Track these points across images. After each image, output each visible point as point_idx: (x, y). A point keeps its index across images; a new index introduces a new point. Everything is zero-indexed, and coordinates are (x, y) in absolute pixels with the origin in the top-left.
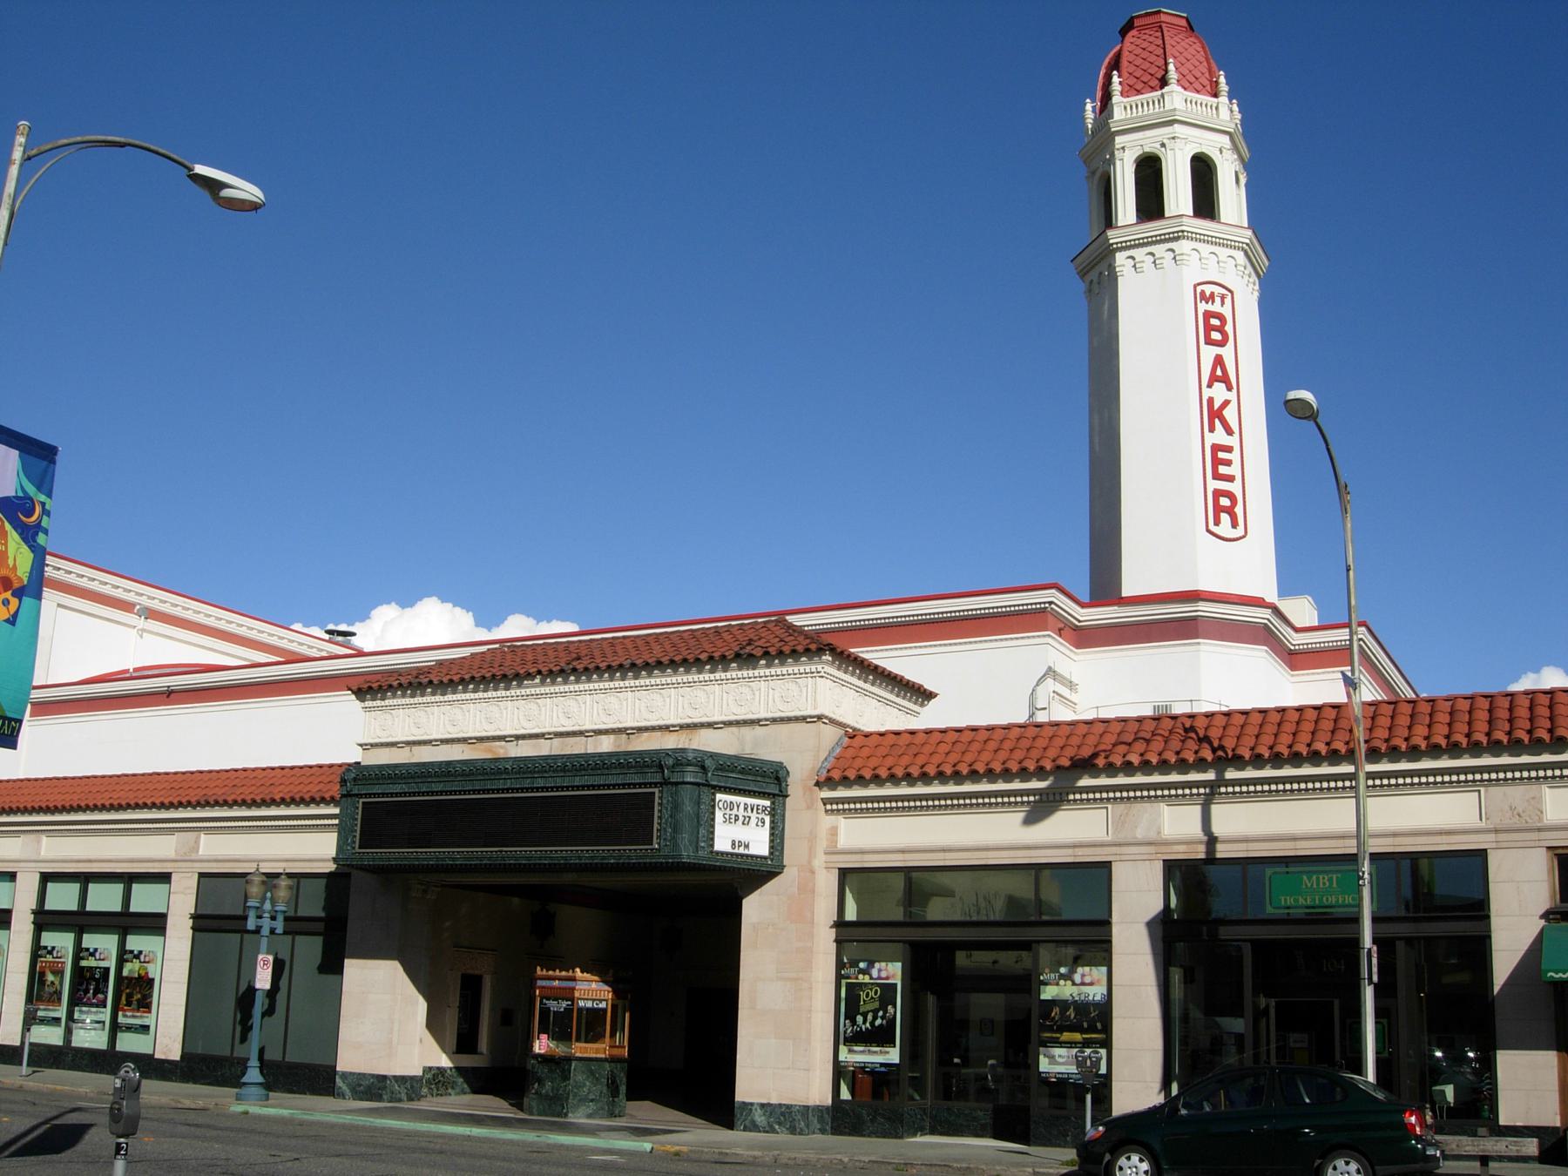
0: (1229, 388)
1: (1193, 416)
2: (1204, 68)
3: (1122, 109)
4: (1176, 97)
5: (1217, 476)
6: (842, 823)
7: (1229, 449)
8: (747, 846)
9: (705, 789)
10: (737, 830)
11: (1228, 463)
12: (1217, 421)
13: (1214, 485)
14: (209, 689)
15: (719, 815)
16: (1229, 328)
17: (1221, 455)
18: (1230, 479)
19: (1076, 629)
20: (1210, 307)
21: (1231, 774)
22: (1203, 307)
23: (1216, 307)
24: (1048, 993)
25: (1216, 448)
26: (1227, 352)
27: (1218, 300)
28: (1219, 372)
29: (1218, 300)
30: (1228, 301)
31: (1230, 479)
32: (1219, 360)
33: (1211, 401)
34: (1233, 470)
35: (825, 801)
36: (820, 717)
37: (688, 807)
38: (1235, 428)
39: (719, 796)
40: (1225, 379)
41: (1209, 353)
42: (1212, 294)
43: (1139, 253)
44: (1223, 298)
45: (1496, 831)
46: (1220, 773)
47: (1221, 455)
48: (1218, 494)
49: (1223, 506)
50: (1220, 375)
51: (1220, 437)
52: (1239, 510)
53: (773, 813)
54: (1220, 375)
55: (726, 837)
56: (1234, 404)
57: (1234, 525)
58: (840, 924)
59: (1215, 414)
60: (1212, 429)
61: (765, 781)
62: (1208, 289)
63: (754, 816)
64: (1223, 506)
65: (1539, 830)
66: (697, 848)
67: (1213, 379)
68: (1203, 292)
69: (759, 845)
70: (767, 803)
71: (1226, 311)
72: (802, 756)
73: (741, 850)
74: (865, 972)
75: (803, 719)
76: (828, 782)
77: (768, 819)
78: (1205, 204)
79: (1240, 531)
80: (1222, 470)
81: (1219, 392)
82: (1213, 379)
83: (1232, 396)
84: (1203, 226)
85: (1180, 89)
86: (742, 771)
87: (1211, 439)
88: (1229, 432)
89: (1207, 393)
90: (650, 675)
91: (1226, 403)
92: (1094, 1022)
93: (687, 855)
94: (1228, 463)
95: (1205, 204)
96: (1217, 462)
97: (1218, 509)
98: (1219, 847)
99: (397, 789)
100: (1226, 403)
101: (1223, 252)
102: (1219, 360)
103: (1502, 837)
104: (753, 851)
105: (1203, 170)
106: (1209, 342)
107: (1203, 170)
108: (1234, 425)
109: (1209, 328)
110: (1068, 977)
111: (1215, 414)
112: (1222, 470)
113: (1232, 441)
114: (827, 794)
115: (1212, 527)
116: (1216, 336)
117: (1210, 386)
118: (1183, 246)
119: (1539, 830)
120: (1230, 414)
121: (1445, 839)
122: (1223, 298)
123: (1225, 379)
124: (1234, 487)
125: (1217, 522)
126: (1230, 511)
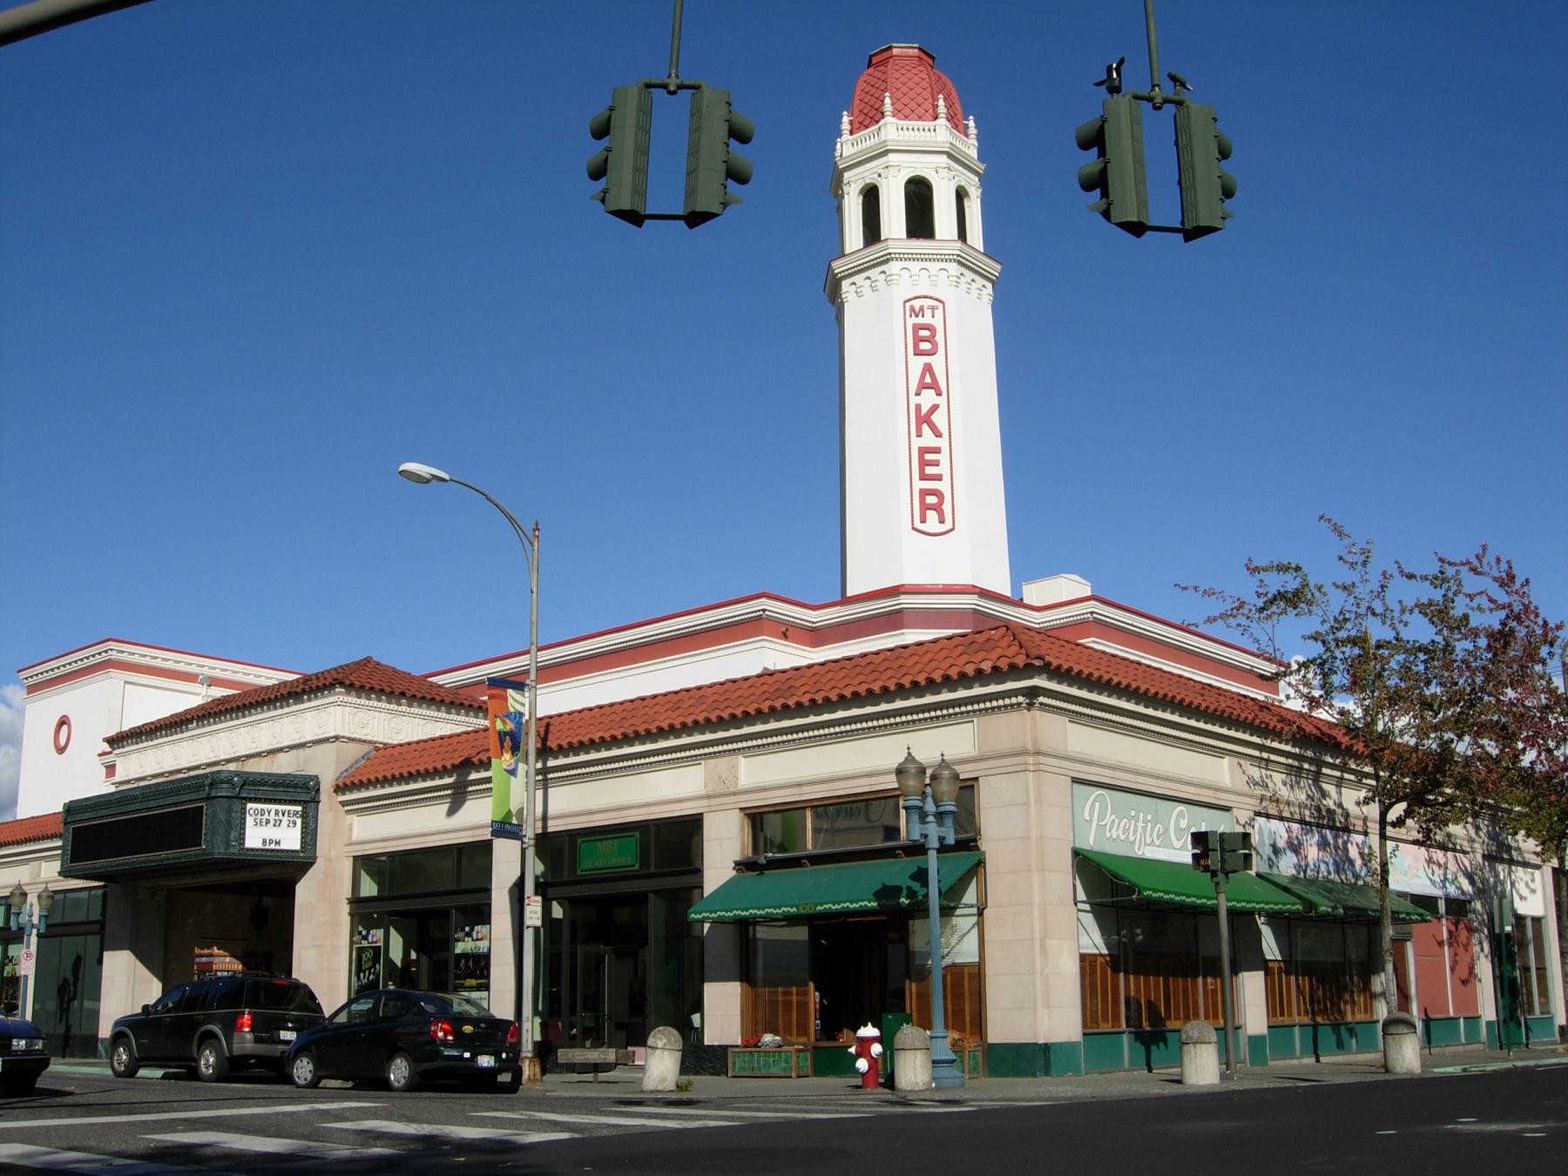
0: (939, 394)
1: (902, 422)
2: (927, 94)
3: (848, 146)
4: (891, 129)
5: (924, 477)
6: (355, 820)
7: (937, 450)
8: (278, 843)
9: (237, 802)
10: (268, 830)
11: (936, 463)
12: (925, 426)
13: (919, 485)
14: (72, 745)
15: (249, 821)
16: (939, 338)
17: (928, 457)
18: (938, 478)
19: (813, 630)
20: (920, 320)
21: (551, 763)
23: (927, 319)
24: (460, 948)
25: (923, 451)
26: (937, 362)
27: (928, 312)
28: (928, 380)
29: (928, 312)
30: (939, 313)
31: (938, 478)
32: (928, 368)
33: (918, 407)
34: (943, 469)
35: (344, 804)
36: (337, 738)
37: (222, 816)
38: (944, 431)
39: (249, 805)
40: (934, 386)
41: (918, 363)
42: (922, 309)
43: (859, 279)
44: (933, 308)
45: (708, 797)
46: (544, 763)
47: (928, 457)
48: (924, 493)
49: (931, 503)
50: (928, 382)
51: (928, 439)
52: (947, 507)
53: (304, 816)
54: (928, 382)
55: (256, 836)
56: (943, 410)
57: (942, 521)
58: (356, 902)
59: (924, 419)
60: (919, 435)
61: (298, 792)
62: (917, 304)
63: (285, 820)
64: (931, 503)
65: (734, 794)
66: (228, 846)
67: (923, 386)
68: (912, 309)
69: (289, 838)
70: (299, 808)
71: (937, 323)
72: (326, 767)
73: (273, 846)
74: (365, 938)
75: (326, 740)
76: (339, 789)
77: (299, 821)
78: (920, 221)
79: (948, 525)
80: (929, 470)
81: (928, 398)
82: (923, 386)
83: (942, 401)
84: (921, 245)
85: (894, 120)
86: (274, 785)
87: (917, 443)
88: (938, 434)
89: (914, 400)
90: (420, 706)
91: (935, 408)
92: (480, 966)
93: (219, 852)
94: (936, 463)
95: (920, 221)
96: (923, 463)
97: (925, 507)
98: (550, 823)
99: (87, 815)
100: (935, 408)
101: (934, 267)
102: (928, 368)
103: (713, 802)
104: (284, 846)
105: (919, 196)
106: (918, 353)
108: (943, 429)
109: (917, 340)
110: (469, 935)
111: (924, 419)
112: (929, 470)
113: (942, 443)
114: (342, 798)
115: (918, 525)
116: (924, 346)
117: (918, 394)
118: (894, 267)
119: (734, 794)
120: (939, 418)
121: (674, 807)
122: (933, 308)
123: (934, 386)
124: (942, 486)
125: (923, 521)
126: (938, 508)
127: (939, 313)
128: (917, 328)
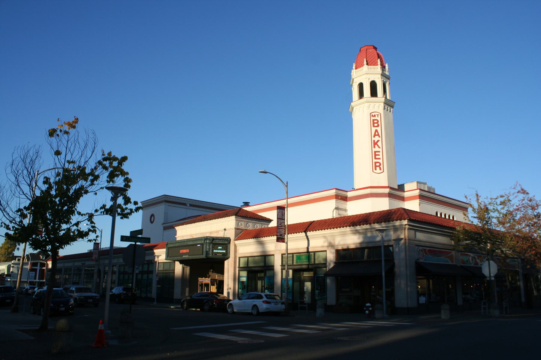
5: (376, 158)
7: (379, 152)
11: (379, 155)
12: (376, 146)
13: (375, 161)
16: (379, 123)
17: (377, 153)
18: (379, 159)
22: (373, 118)
25: (375, 152)
26: (379, 129)
30: (379, 116)
31: (379, 159)
32: (376, 131)
33: (374, 141)
34: (381, 157)
40: (378, 135)
41: (374, 129)
44: (378, 115)
47: (377, 153)
48: (376, 163)
51: (377, 149)
52: (381, 166)
54: (376, 134)
57: (380, 169)
60: (374, 147)
62: (373, 114)
64: (376, 166)
71: (379, 119)
78: (374, 93)
79: (382, 171)
80: (377, 157)
81: (376, 139)
83: (380, 139)
84: (374, 99)
87: (374, 150)
88: (379, 147)
89: (373, 139)
91: (378, 141)
94: (379, 155)
95: (374, 93)
96: (375, 155)
97: (376, 166)
100: (378, 141)
102: (376, 131)
106: (374, 126)
107: (373, 85)
109: (374, 123)
112: (377, 157)
113: (380, 150)
120: (379, 144)
124: (381, 161)
125: (376, 169)
127: (379, 116)
128: (374, 120)
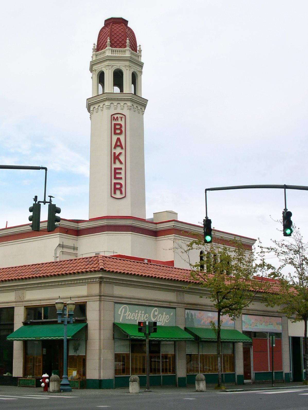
5: (115, 178)
7: (121, 169)
11: (120, 173)
13: (114, 181)
16: (123, 129)
17: (118, 171)
18: (121, 178)
22: (114, 122)
23: (119, 122)
25: (115, 169)
26: (122, 137)
27: (119, 119)
28: (119, 144)
29: (119, 119)
30: (123, 119)
31: (121, 178)
32: (118, 139)
33: (115, 153)
34: (123, 176)
40: (121, 146)
42: (117, 117)
47: (118, 171)
48: (115, 184)
50: (118, 144)
51: (118, 165)
52: (123, 189)
54: (118, 144)
57: (121, 193)
60: (115, 163)
67: (116, 146)
68: (114, 117)
71: (123, 123)
79: (124, 196)
80: (118, 176)
81: (118, 150)
83: (123, 151)
87: (114, 166)
88: (121, 163)
94: (120, 173)
96: (116, 173)
97: (115, 189)
100: (120, 154)
102: (118, 139)
103: (17, 303)
106: (115, 133)
109: (115, 129)
111: (116, 158)
112: (118, 176)
113: (123, 166)
115: (113, 195)
117: (115, 148)
120: (122, 158)
123: (121, 146)
124: (122, 182)
125: (115, 193)
126: (120, 189)
127: (123, 119)
128: (115, 125)
